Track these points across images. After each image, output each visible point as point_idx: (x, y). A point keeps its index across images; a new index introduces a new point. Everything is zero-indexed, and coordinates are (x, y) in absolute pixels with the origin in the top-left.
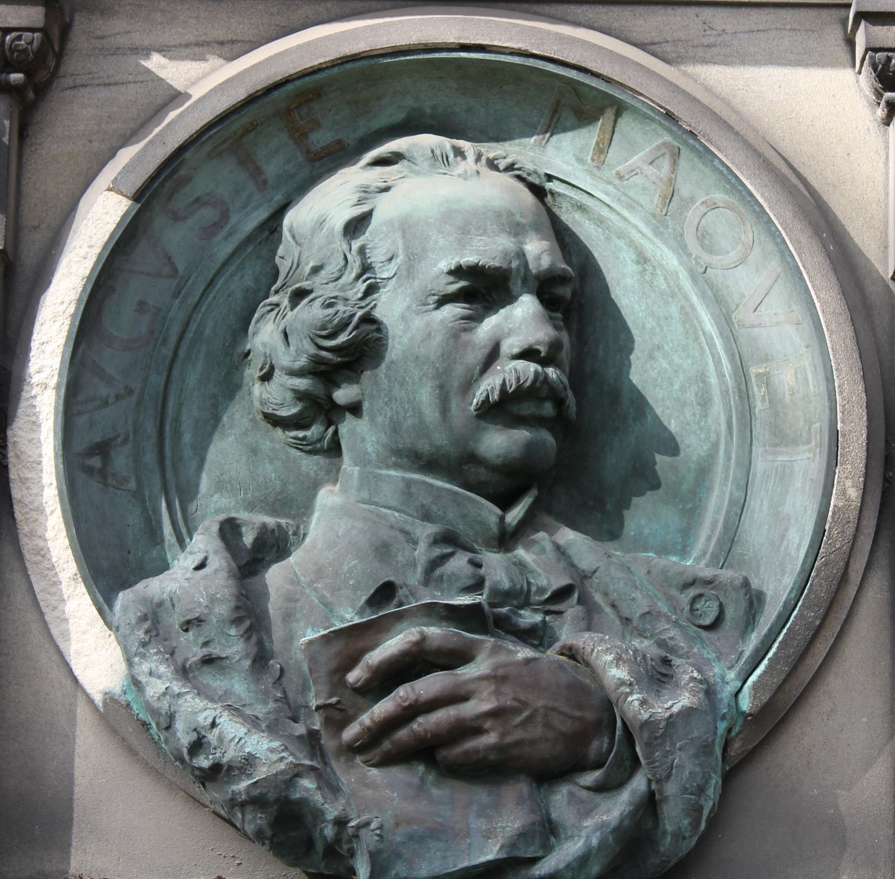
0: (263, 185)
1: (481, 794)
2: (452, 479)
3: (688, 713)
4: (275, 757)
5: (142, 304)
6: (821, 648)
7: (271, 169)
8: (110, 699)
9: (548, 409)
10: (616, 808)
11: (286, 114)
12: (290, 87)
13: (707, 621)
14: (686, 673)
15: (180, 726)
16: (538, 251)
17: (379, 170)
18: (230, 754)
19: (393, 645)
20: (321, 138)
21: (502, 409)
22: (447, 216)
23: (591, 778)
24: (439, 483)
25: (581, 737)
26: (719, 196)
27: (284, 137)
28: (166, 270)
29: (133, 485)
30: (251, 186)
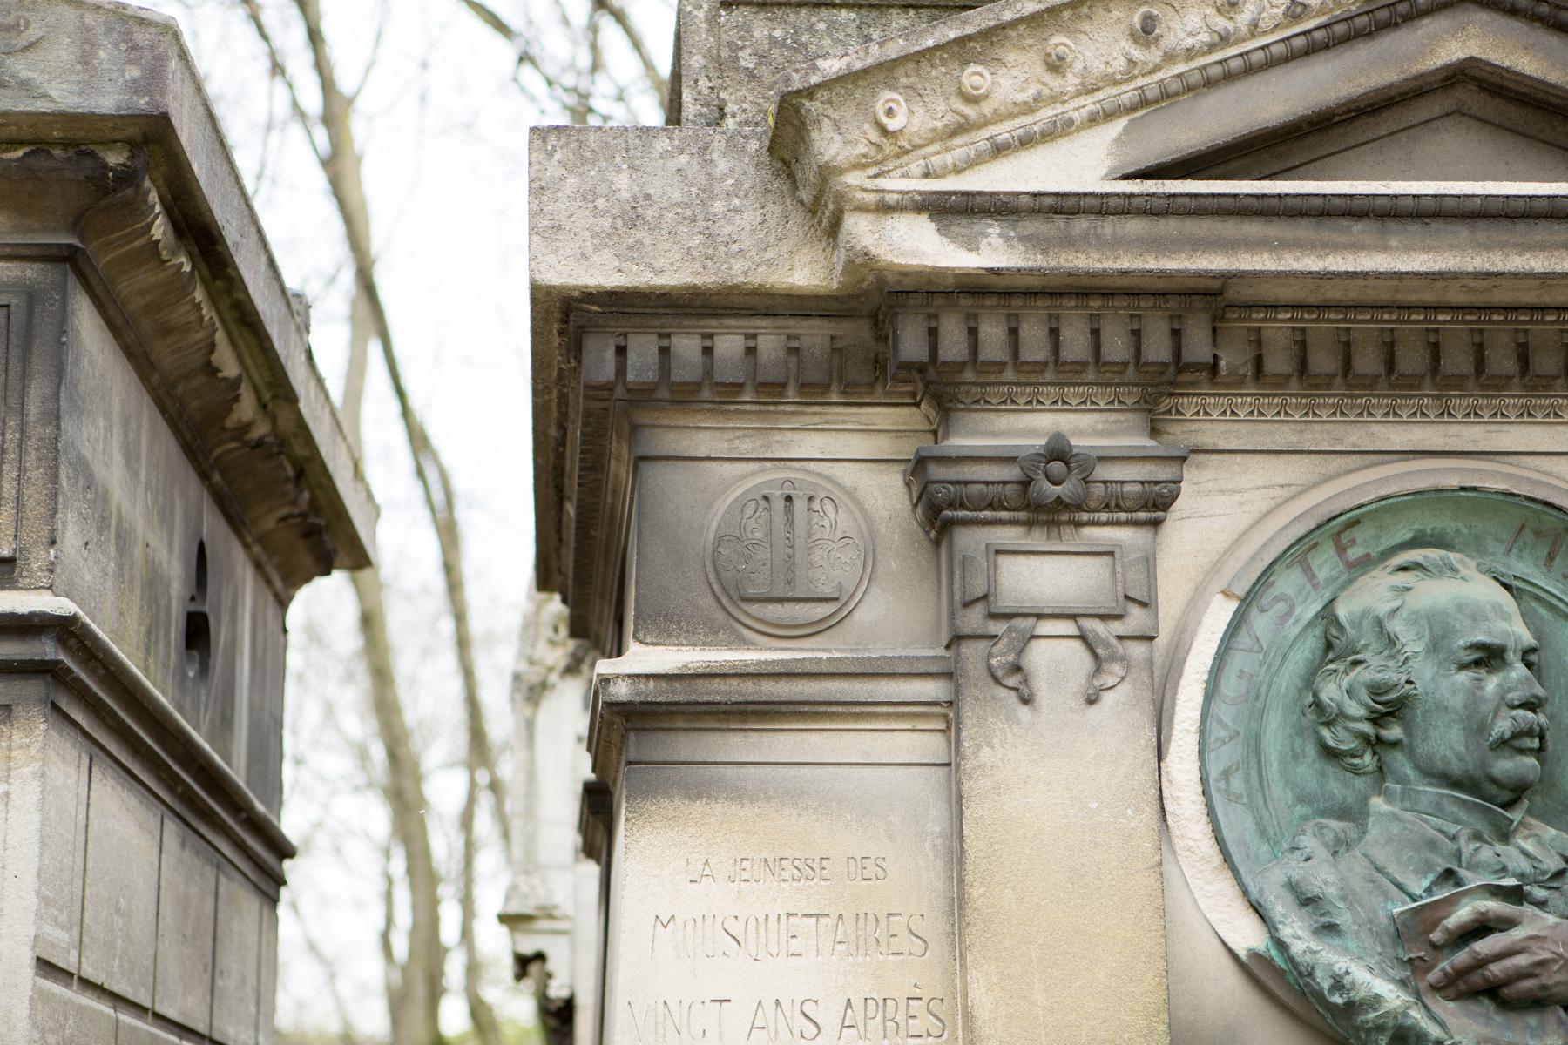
0: (1315, 586)
1: (1532, 1020)
2: (1471, 794)
4: (1393, 996)
5: (1242, 671)
7: (1322, 575)
8: (1254, 955)
9: (1536, 743)
11: (1336, 537)
12: (1343, 518)
15: (1319, 974)
17: (1402, 575)
18: (1359, 995)
19: (1463, 914)
20: (1354, 553)
21: (1506, 744)
27: (1332, 552)
28: (1256, 648)
29: (1245, 800)
30: (1309, 586)
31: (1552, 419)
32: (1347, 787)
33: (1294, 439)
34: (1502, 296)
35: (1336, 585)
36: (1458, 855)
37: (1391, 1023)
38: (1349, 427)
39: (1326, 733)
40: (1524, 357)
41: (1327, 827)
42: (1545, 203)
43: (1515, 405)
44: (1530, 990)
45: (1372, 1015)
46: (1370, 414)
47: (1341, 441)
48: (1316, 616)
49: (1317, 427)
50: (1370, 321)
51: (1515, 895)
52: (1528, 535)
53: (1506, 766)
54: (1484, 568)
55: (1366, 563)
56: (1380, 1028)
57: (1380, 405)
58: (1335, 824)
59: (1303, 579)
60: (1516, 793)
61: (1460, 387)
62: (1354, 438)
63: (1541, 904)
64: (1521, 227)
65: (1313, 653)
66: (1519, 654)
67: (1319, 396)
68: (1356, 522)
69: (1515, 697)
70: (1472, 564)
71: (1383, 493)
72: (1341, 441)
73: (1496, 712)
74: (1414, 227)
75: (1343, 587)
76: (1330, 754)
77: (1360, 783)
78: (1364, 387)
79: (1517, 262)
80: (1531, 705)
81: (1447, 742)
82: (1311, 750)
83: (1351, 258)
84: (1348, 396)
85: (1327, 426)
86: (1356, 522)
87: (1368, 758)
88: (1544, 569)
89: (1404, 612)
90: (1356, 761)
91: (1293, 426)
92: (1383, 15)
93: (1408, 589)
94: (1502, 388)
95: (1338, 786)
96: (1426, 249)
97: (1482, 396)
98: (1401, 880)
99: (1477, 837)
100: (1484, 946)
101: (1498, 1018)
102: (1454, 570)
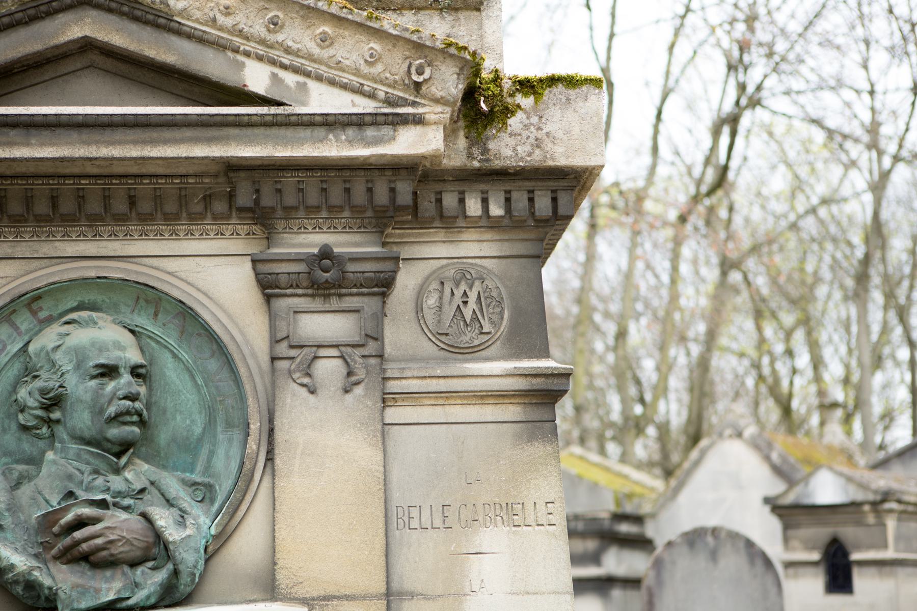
0: (20, 334)
1: (108, 573)
2: (97, 448)
3: (189, 536)
4: (22, 564)
6: (244, 508)
7: (23, 327)
9: (135, 418)
10: (161, 576)
11: (29, 305)
12: (28, 295)
13: (199, 499)
14: (190, 521)
16: (134, 356)
17: (67, 326)
19: (70, 517)
20: (42, 315)
21: (116, 419)
22: (93, 344)
23: (150, 564)
24: (92, 450)
25: (147, 549)
26: (202, 332)
27: (28, 314)
30: (15, 334)
31: (174, 237)
32: (33, 446)
33: (10, 251)
34: (118, 169)
35: (32, 332)
36: (82, 482)
37: (21, 579)
38: (42, 244)
39: (21, 417)
40: (132, 201)
41: (14, 469)
42: (119, 118)
43: (136, 230)
44: (105, 557)
45: (11, 575)
46: (54, 236)
47: (37, 252)
48: (20, 350)
49: (24, 244)
50: (43, 184)
51: (103, 504)
52: (142, 302)
53: (114, 432)
54: (117, 321)
55: (50, 320)
56: (16, 582)
57: (58, 232)
58: (21, 467)
59: (11, 330)
60: (124, 448)
61: (102, 220)
62: (45, 250)
63: (127, 509)
64: (108, 132)
65: (19, 371)
66: (129, 370)
67: (21, 227)
68: (39, 298)
69: (121, 393)
70: (110, 318)
71: (51, 281)
72: (37, 252)
73: (110, 402)
74: (46, 133)
75: (36, 334)
76: (25, 428)
77: (41, 444)
78: (47, 221)
79: (104, 151)
80: (133, 398)
81: (81, 419)
82: (14, 427)
83: (7, 150)
84: (38, 226)
85: (30, 243)
86: (39, 298)
87: (45, 430)
88: (153, 321)
89: (63, 348)
90: (38, 432)
91: (9, 244)
92: (32, 12)
93: (68, 335)
94: (127, 220)
95: (28, 446)
96: (52, 145)
97: (116, 225)
98: (48, 498)
99: (96, 472)
100: (78, 534)
101: (89, 573)
102: (96, 323)
